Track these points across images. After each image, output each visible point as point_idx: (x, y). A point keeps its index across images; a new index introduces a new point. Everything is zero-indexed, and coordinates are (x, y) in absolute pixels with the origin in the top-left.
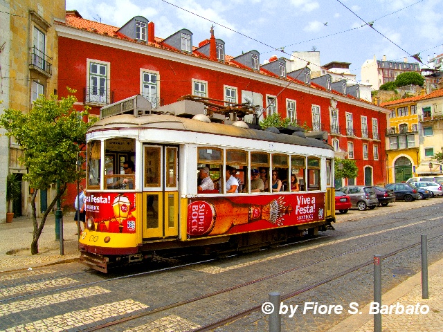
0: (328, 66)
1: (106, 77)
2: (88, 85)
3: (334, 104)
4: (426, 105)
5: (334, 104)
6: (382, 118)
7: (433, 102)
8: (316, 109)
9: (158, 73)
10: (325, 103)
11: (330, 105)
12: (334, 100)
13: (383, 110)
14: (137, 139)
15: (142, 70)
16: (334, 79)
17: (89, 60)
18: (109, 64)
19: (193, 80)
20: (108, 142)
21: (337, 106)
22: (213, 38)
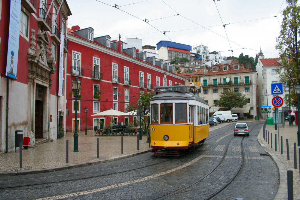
0: (144, 47)
1: (80, 61)
2: (72, 66)
3: (165, 76)
4: (205, 78)
5: (165, 76)
6: (183, 82)
7: (208, 78)
8: (158, 79)
9: (99, 59)
10: (161, 75)
11: (164, 76)
12: (165, 74)
13: (184, 79)
14: (188, 104)
15: (93, 57)
16: (148, 55)
17: (73, 51)
18: (81, 53)
19: (113, 63)
20: (161, 104)
21: (167, 77)
22: (120, 41)
